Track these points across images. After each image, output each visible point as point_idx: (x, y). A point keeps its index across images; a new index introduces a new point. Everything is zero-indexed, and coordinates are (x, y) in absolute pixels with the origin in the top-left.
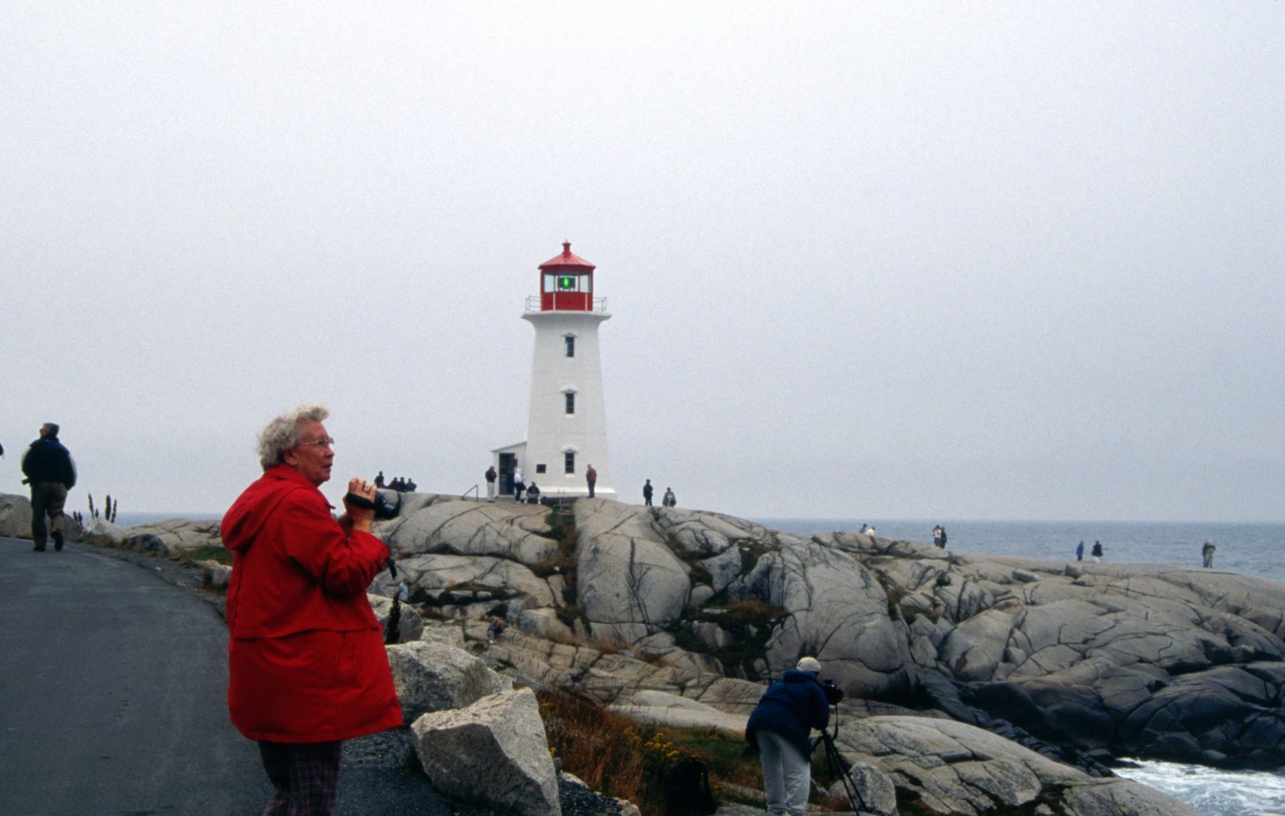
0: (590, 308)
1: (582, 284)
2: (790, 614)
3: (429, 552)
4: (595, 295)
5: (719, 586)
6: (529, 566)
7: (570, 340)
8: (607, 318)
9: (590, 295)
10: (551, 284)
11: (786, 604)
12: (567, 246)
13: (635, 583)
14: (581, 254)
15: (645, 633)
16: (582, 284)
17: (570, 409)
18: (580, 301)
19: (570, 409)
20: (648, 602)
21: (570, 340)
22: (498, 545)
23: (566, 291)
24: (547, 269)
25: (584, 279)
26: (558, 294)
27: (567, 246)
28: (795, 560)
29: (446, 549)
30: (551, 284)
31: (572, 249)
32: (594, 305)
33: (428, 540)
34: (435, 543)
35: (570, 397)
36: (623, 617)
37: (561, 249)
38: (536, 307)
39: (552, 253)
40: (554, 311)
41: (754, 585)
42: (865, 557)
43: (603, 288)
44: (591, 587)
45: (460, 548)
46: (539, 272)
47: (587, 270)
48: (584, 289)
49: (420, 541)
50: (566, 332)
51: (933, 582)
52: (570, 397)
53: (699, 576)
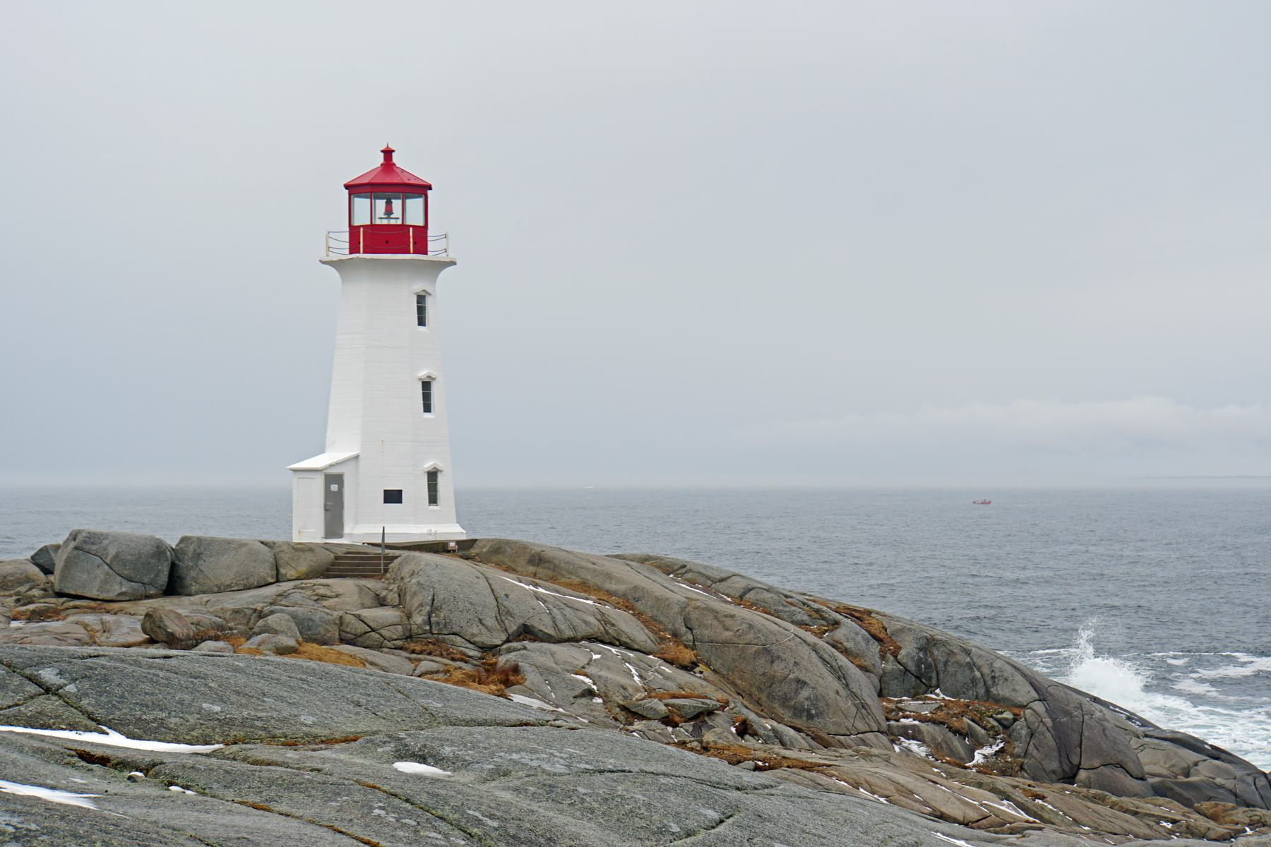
0: (422, 248)
1: (413, 212)
2: (1024, 707)
4: (431, 232)
7: (421, 300)
10: (366, 211)
11: (1001, 690)
12: (388, 153)
13: (840, 674)
14: (409, 164)
16: (413, 212)
21: (421, 300)
22: (585, 622)
23: (389, 225)
25: (415, 205)
27: (388, 153)
29: (527, 632)
30: (366, 211)
31: (396, 159)
32: (431, 246)
33: (500, 622)
34: (513, 628)
35: (426, 386)
36: (861, 726)
37: (380, 159)
41: (919, 663)
44: (801, 683)
45: (551, 631)
46: (347, 191)
48: (414, 218)
50: (418, 287)
52: (426, 386)
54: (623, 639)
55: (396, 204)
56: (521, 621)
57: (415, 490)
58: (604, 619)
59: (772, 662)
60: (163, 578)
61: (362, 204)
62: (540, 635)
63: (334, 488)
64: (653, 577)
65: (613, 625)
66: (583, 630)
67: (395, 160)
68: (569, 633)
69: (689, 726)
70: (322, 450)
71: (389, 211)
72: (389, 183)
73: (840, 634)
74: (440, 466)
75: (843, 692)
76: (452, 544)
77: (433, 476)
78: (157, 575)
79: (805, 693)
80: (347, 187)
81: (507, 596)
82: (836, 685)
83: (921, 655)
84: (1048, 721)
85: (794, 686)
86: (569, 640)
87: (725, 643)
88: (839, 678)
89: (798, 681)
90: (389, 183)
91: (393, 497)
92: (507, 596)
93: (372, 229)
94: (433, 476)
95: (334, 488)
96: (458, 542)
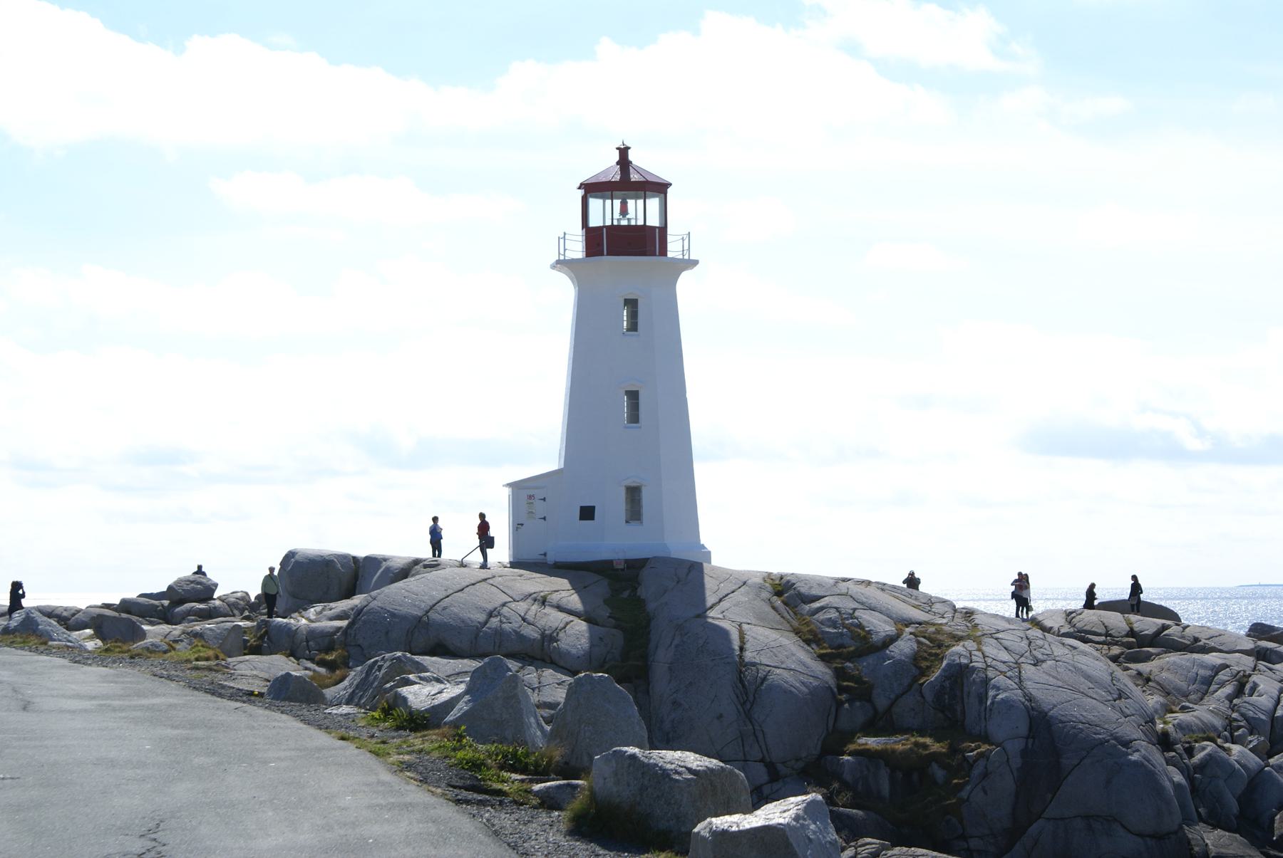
4: (669, 231)
5: (881, 702)
8: (693, 263)
9: (663, 230)
12: (624, 152)
14: (646, 162)
15: (765, 778)
17: (634, 417)
18: (646, 242)
19: (634, 417)
24: (592, 189)
25: (653, 204)
26: (612, 229)
27: (624, 152)
28: (1005, 656)
30: (603, 212)
31: (632, 156)
32: (669, 248)
38: (576, 249)
39: (604, 164)
42: (1116, 650)
43: (685, 221)
46: (581, 192)
47: (659, 188)
48: (654, 221)
51: (1228, 689)
52: (633, 396)
55: (631, 203)
57: (612, 506)
61: (595, 204)
67: (631, 158)
71: (624, 211)
72: (626, 182)
77: (634, 494)
83: (947, 684)
84: (1017, 762)
89: (674, 703)
90: (626, 182)
91: (587, 513)
93: (613, 230)
94: (634, 494)
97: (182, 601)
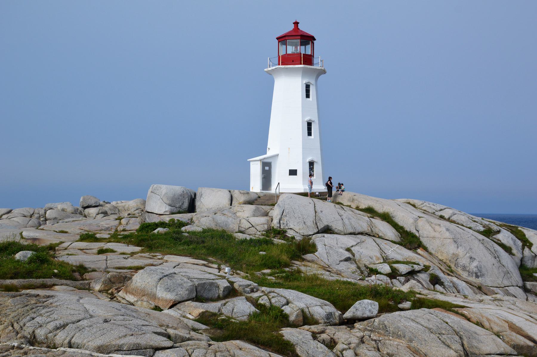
3: (318, 233)
5: (520, 256)
6: (394, 242)
7: (308, 87)
12: (296, 24)
20: (512, 270)
24: (282, 39)
27: (296, 24)
29: (327, 230)
31: (300, 26)
34: (321, 226)
35: (309, 124)
36: (506, 283)
37: (292, 27)
40: (302, 66)
46: (277, 41)
49: (310, 223)
52: (309, 124)
53: (508, 250)
54: (380, 234)
56: (326, 224)
58: (371, 225)
59: (458, 247)
60: (186, 205)
62: (336, 231)
63: (267, 168)
64: (406, 208)
65: (376, 227)
66: (360, 230)
67: (299, 27)
68: (351, 231)
69: (402, 279)
70: (266, 154)
73: (499, 236)
74: (315, 160)
75: (497, 265)
76: (317, 193)
78: (183, 204)
79: (475, 264)
80: (277, 39)
81: (322, 211)
82: (494, 261)
85: (469, 260)
86: (351, 234)
87: (434, 238)
88: (495, 258)
91: (293, 172)
92: (322, 211)
94: (311, 164)
95: (267, 168)
96: (319, 193)
97: (89, 207)
